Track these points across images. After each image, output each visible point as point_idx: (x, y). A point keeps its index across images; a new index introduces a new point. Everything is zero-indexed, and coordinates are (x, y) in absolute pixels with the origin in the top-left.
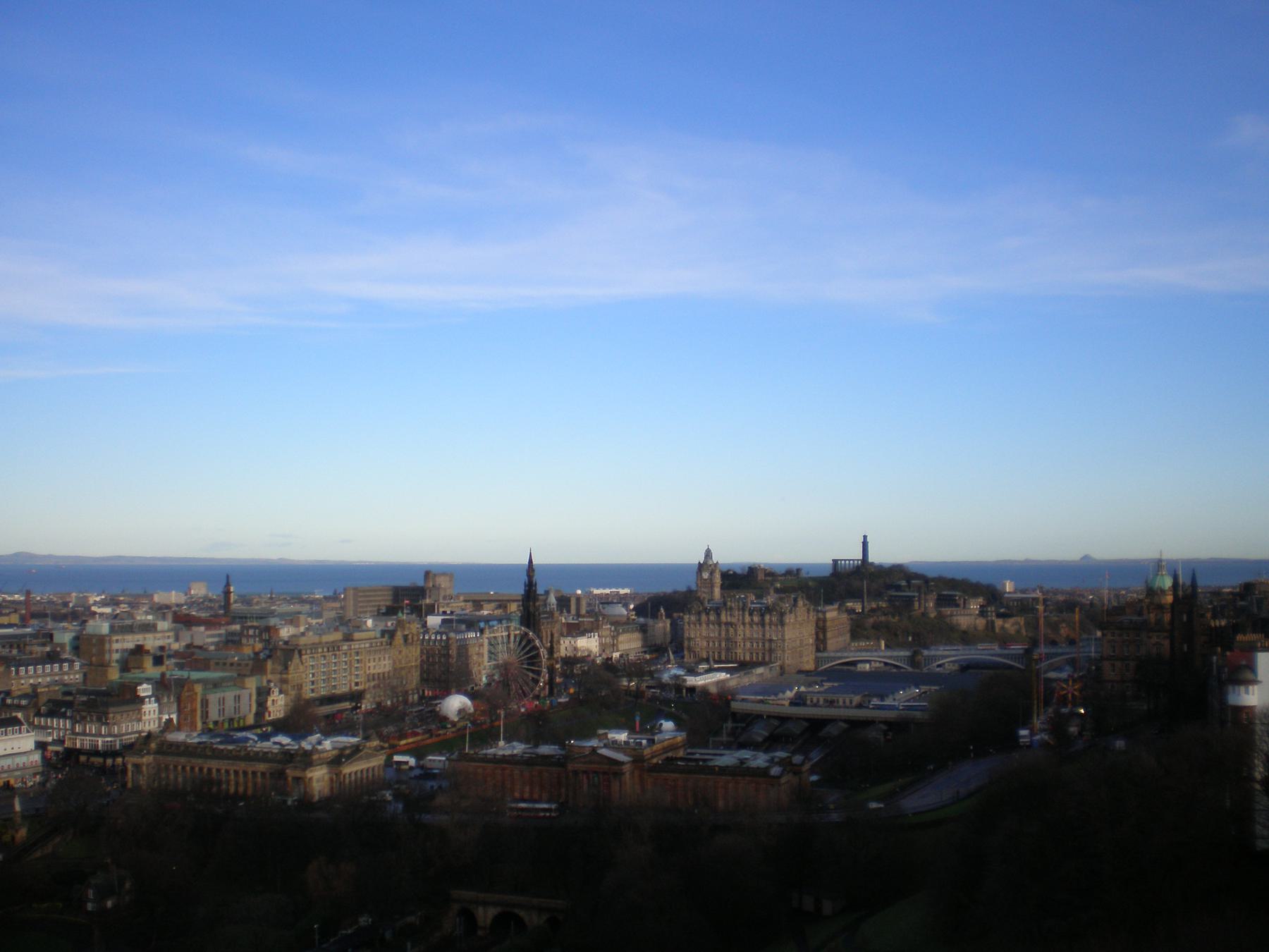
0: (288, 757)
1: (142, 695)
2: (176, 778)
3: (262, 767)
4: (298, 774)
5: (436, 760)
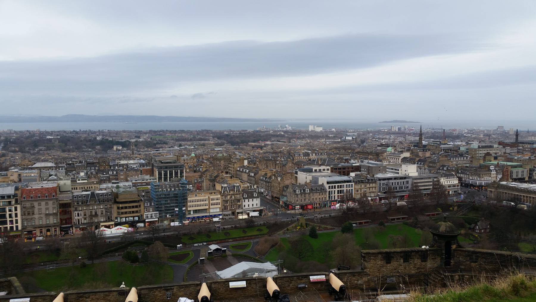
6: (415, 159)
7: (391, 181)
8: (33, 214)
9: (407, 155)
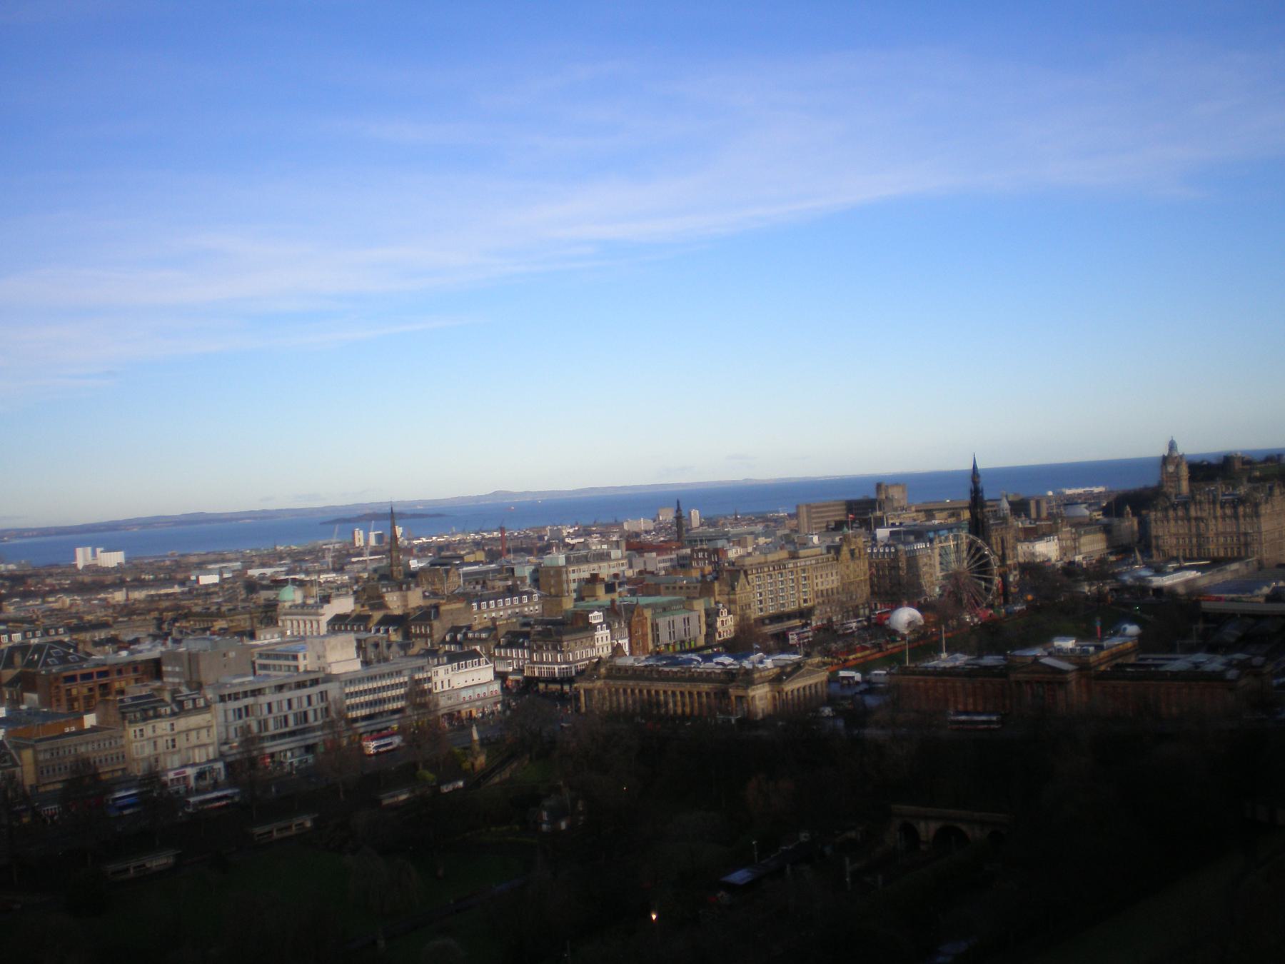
0: (730, 676)
1: (594, 622)
2: (618, 700)
3: (705, 687)
4: (740, 693)
5: (879, 673)
6: (370, 617)
7: (263, 700)
9: (344, 605)
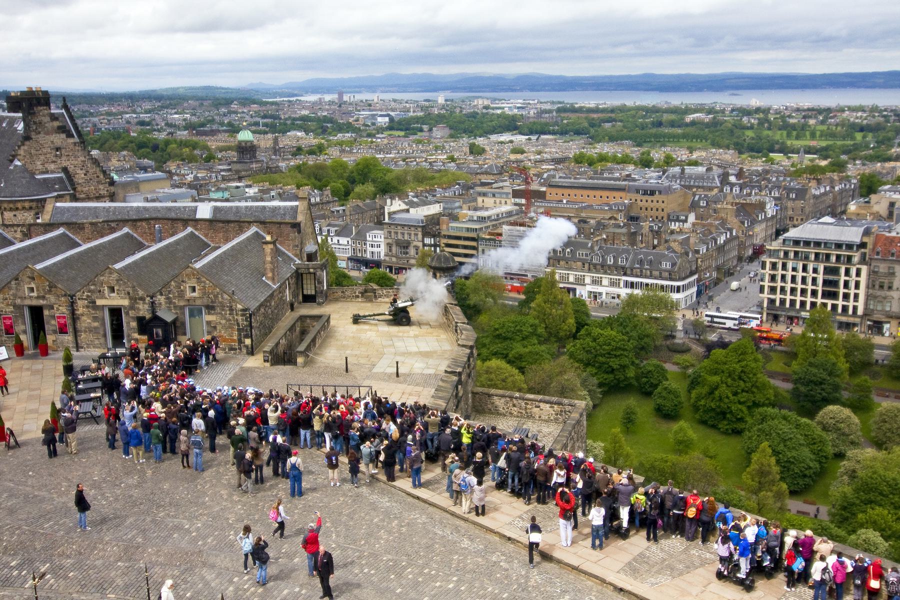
8: (890, 288)
